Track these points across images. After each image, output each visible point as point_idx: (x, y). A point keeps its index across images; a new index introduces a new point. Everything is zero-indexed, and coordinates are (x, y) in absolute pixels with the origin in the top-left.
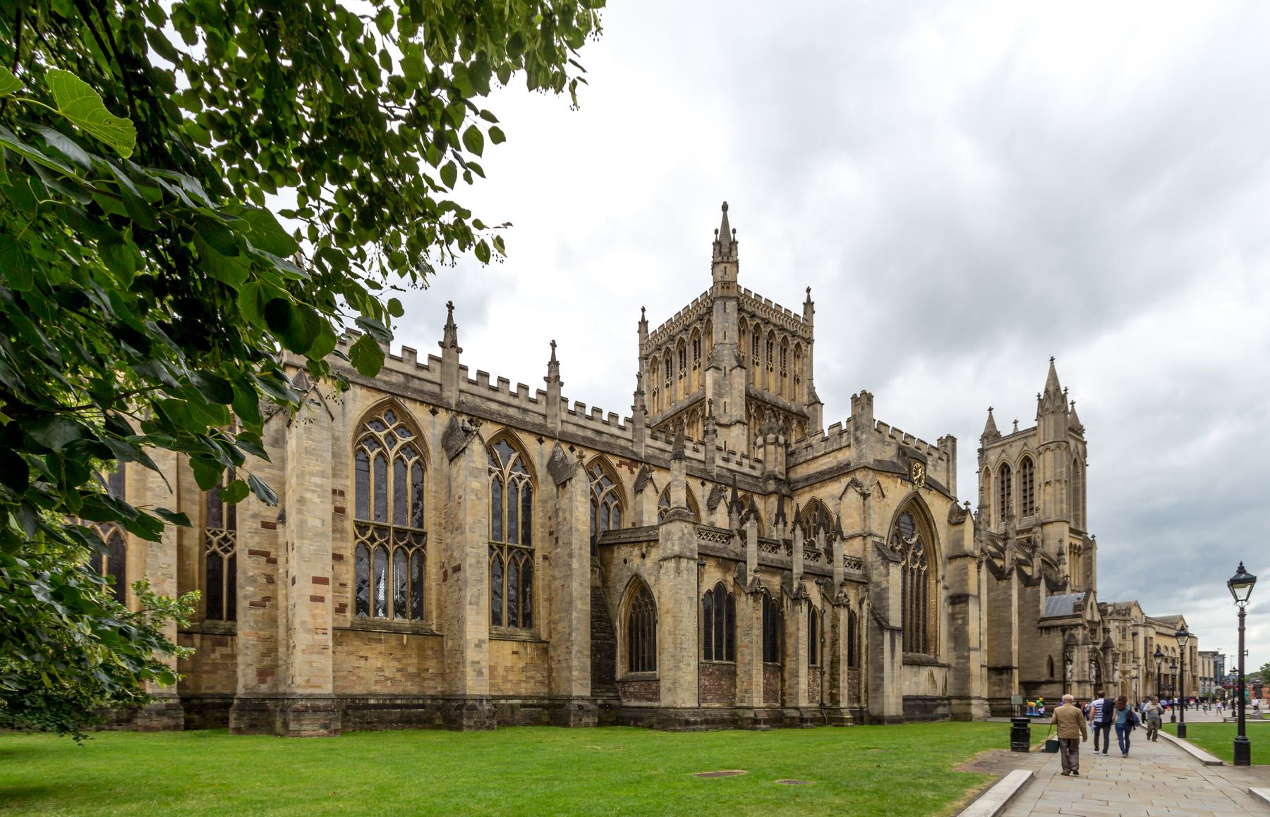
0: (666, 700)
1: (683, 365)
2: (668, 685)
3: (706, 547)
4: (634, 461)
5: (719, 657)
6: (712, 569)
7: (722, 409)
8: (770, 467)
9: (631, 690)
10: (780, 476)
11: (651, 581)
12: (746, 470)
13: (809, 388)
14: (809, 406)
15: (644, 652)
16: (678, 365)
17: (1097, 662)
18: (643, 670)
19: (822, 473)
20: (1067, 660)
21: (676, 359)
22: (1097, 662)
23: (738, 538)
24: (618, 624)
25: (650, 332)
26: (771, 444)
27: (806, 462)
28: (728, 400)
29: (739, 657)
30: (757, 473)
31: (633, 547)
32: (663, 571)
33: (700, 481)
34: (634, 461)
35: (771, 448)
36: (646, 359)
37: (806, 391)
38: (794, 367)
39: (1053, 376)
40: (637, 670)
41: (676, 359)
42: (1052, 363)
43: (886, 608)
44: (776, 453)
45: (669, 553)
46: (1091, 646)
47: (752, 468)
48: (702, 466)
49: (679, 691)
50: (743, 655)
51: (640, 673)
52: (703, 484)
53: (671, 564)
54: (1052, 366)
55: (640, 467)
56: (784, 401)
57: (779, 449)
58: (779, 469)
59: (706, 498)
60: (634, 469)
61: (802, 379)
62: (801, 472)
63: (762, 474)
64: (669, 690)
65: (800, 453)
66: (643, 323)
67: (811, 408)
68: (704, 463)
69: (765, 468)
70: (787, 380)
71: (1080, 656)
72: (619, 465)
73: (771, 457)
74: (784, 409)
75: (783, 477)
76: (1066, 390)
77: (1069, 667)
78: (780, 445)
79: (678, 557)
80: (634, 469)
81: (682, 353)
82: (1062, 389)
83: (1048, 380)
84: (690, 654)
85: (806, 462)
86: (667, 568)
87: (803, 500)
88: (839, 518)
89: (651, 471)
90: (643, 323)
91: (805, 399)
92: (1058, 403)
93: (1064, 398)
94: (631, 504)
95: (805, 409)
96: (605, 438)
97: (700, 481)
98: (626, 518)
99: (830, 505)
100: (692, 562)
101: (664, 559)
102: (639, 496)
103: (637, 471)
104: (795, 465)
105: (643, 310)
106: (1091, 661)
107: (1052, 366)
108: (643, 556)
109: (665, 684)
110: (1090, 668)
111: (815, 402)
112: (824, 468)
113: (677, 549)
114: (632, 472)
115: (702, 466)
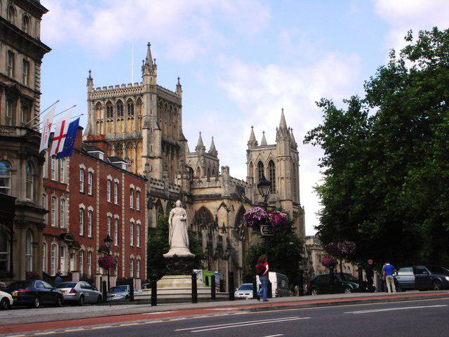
14: (180, 141)
19: (207, 196)
30: (178, 192)
35: (185, 181)
36: (93, 101)
43: (237, 259)
47: (177, 189)
58: (186, 190)
66: (90, 80)
67: (181, 142)
74: (171, 144)
85: (200, 188)
87: (198, 206)
88: (217, 218)
90: (90, 80)
99: (213, 212)
105: (90, 72)
112: (207, 193)
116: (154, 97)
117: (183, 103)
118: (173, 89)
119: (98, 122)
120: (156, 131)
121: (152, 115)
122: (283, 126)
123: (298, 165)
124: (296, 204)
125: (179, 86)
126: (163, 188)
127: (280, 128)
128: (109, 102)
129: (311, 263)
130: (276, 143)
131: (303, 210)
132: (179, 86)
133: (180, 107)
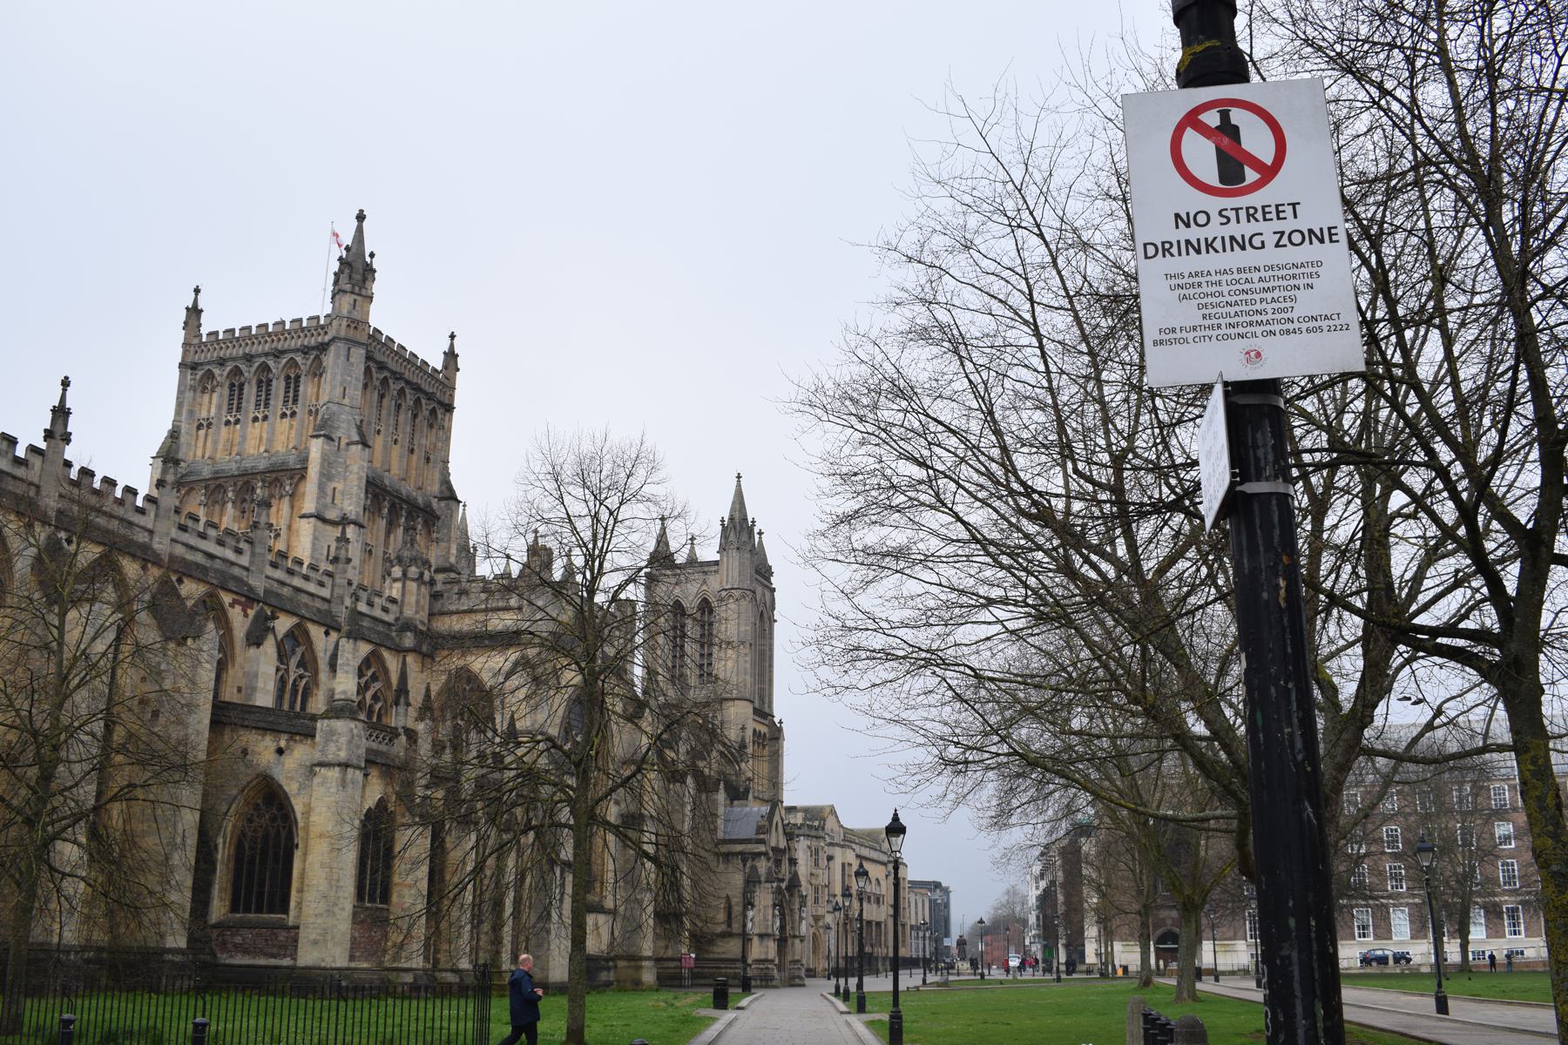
0: (307, 957)
1: (264, 401)
2: (313, 937)
3: (377, 753)
4: (248, 598)
5: (372, 900)
6: (374, 780)
7: (329, 500)
8: (409, 612)
9: (238, 940)
10: (420, 627)
11: (291, 788)
12: (378, 613)
13: (442, 474)
14: (441, 499)
15: (261, 885)
16: (253, 399)
17: (781, 906)
18: (259, 910)
20: (748, 904)
21: (250, 392)
22: (781, 906)
23: (403, 738)
24: (220, 841)
25: (204, 331)
26: (413, 580)
27: (457, 612)
28: (340, 486)
29: (395, 898)
30: (389, 618)
31: (263, 736)
32: (317, 780)
33: (323, 630)
34: (248, 598)
35: (412, 586)
37: (437, 476)
38: (425, 440)
39: (739, 501)
40: (247, 910)
41: (250, 392)
42: (739, 481)
44: (418, 594)
45: (330, 758)
46: (775, 885)
47: (385, 610)
48: (325, 606)
49: (330, 945)
50: (401, 896)
51: (251, 916)
52: (327, 633)
53: (334, 773)
54: (739, 485)
55: (257, 607)
56: (407, 489)
57: (423, 589)
59: (329, 654)
60: (249, 611)
61: (437, 458)
62: (446, 625)
63: (397, 619)
64: (315, 942)
65: (449, 598)
66: (194, 312)
67: (443, 504)
68: (328, 601)
69: (401, 612)
70: (415, 457)
71: (764, 897)
72: (232, 605)
73: (411, 599)
74: (408, 502)
75: (425, 629)
76: (753, 522)
77: (750, 914)
78: (424, 583)
79: (345, 766)
80: (249, 611)
81: (264, 385)
82: (750, 520)
83: (734, 503)
84: (346, 895)
85: (457, 612)
86: (325, 778)
89: (274, 618)
90: (194, 312)
91: (435, 488)
92: (744, 537)
93: (750, 530)
94: (239, 659)
95: (435, 503)
96: (218, 564)
97: (323, 630)
98: (230, 679)
100: (358, 772)
101: (321, 764)
102: (253, 651)
103: (251, 613)
104: (442, 613)
106: (775, 905)
107: (739, 485)
108: (280, 751)
109: (306, 935)
110: (774, 916)
111: (450, 496)
113: (343, 755)
114: (246, 615)
115: (325, 606)
116: (358, 354)
117: (459, 400)
118: (436, 362)
119: (199, 427)
120: (353, 448)
121: (346, 401)
122: (737, 515)
123: (772, 621)
124: (763, 713)
125: (451, 356)
126: (325, 593)
127: (731, 519)
128: (237, 372)
129: (793, 862)
130: (717, 557)
131: (780, 730)
132: (451, 356)
133: (449, 408)
